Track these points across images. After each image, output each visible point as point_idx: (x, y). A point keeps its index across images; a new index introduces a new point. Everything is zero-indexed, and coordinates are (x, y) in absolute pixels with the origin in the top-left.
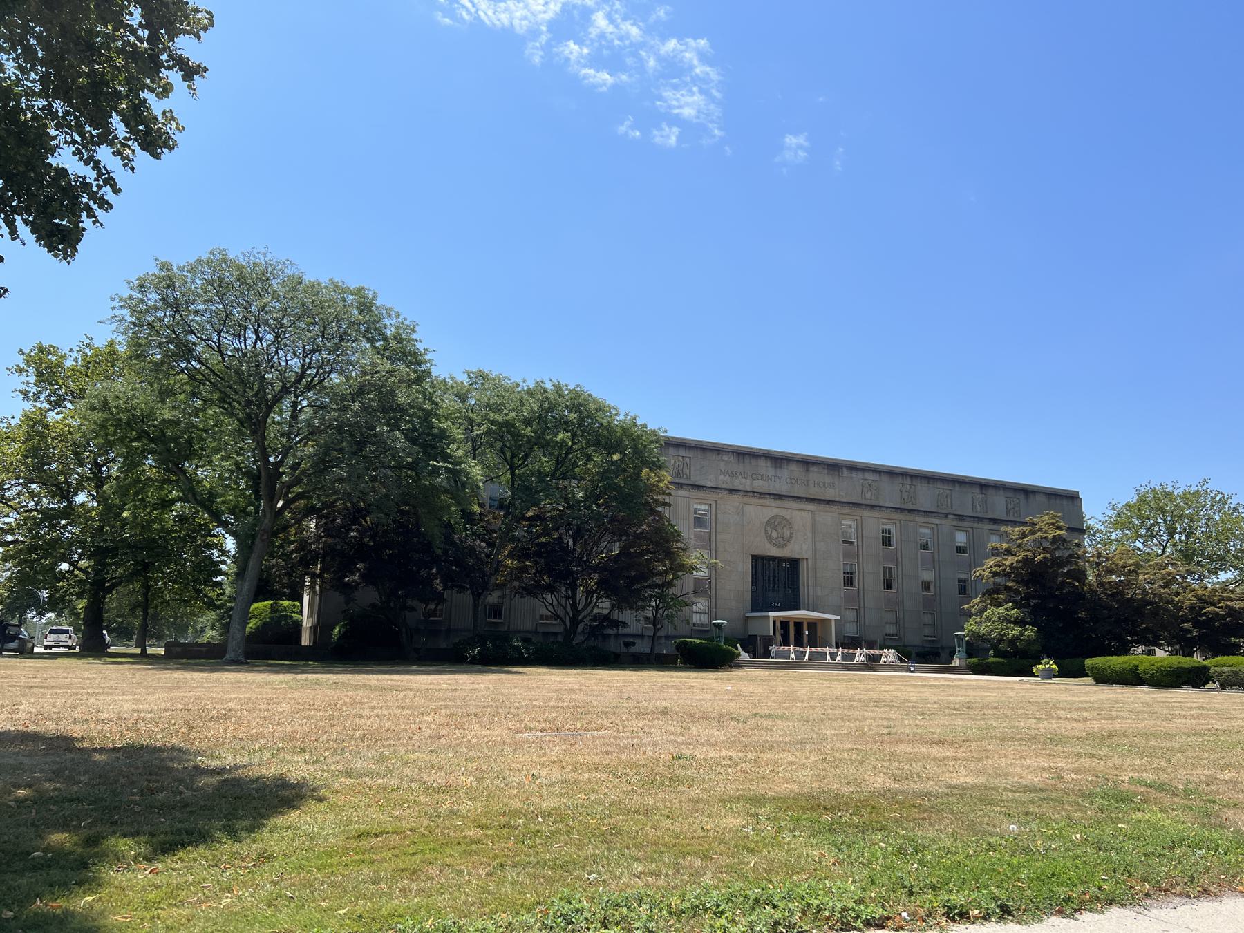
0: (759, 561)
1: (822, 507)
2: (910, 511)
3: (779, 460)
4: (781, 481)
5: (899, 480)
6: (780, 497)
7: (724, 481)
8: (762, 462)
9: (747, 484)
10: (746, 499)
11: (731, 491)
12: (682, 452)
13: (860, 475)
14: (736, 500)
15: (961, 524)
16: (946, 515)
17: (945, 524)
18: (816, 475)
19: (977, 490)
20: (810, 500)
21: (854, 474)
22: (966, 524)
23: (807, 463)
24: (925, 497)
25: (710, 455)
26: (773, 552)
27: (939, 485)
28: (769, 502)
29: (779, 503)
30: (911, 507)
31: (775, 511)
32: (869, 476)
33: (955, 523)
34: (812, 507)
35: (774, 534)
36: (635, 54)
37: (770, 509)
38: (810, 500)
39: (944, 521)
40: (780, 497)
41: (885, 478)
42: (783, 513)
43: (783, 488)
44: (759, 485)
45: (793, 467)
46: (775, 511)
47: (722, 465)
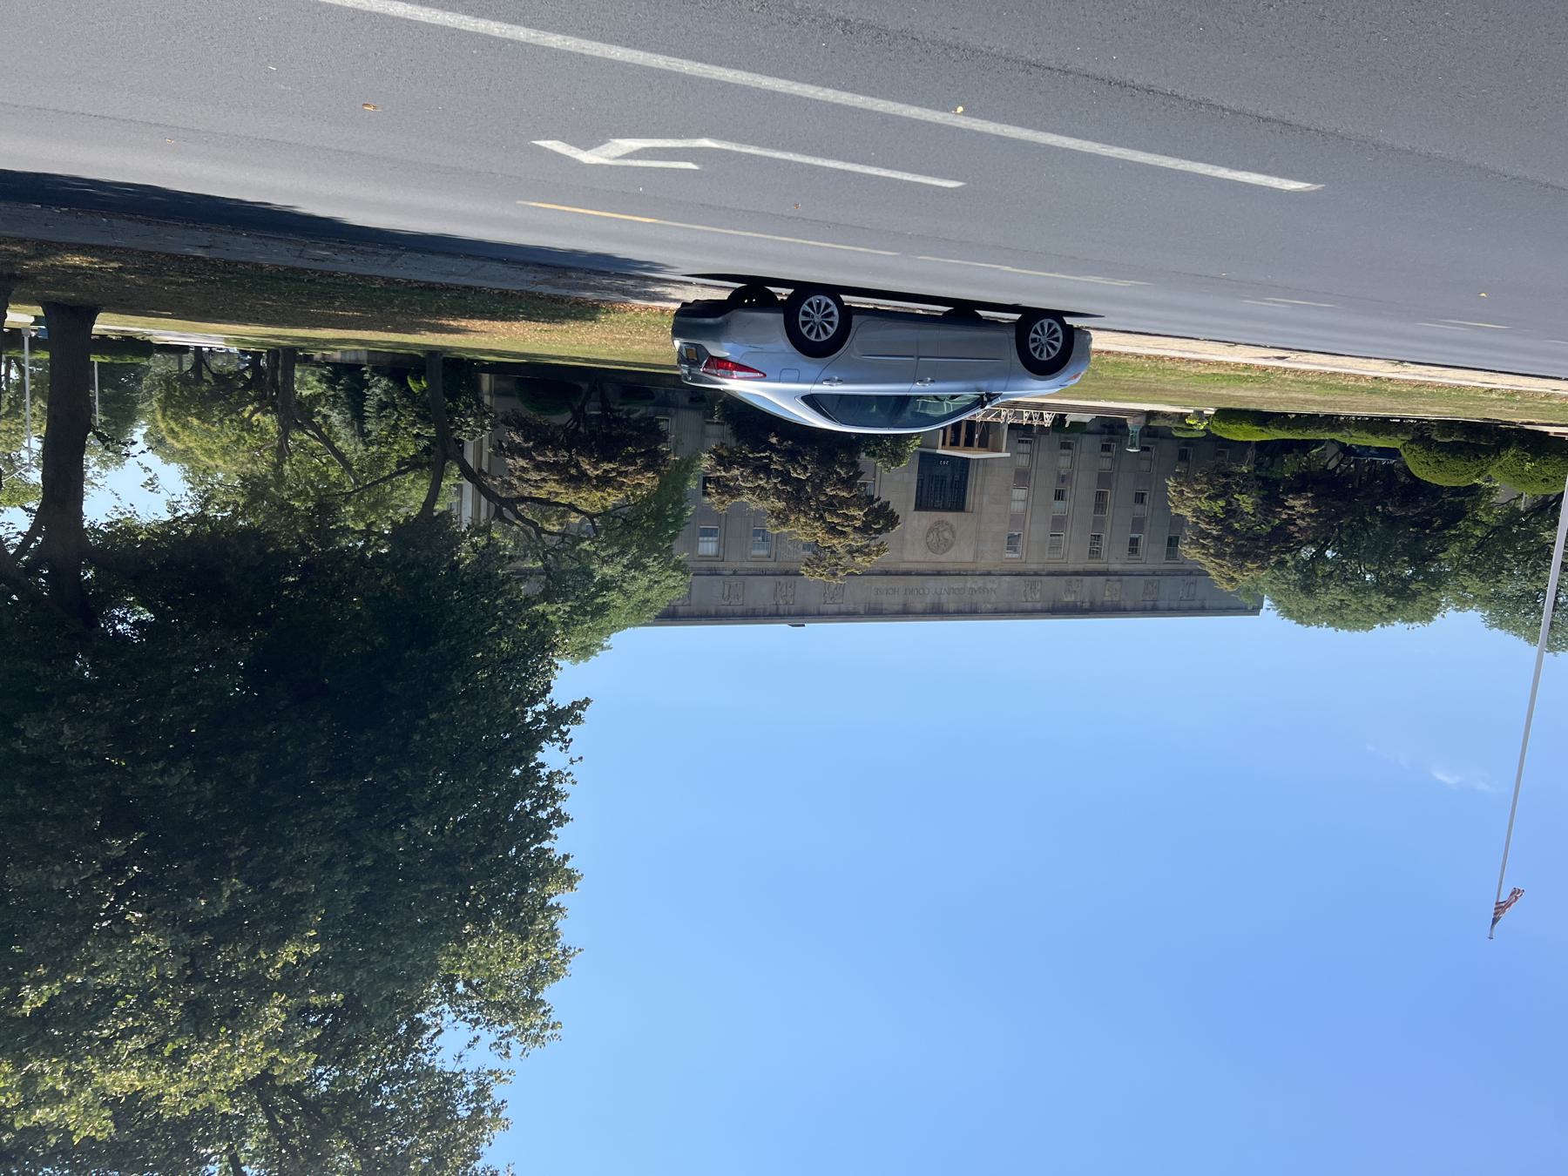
0: (958, 505)
1: (892, 568)
2: (787, 573)
3: (937, 612)
4: (934, 589)
5: (793, 609)
6: (939, 574)
7: (992, 583)
8: (952, 607)
9: (971, 583)
10: (973, 567)
11: (989, 574)
12: (1029, 606)
13: (843, 608)
14: (983, 565)
15: (713, 565)
16: (735, 573)
17: (734, 562)
18: (895, 601)
19: (681, 609)
20: (907, 573)
21: (851, 607)
22: (705, 565)
23: (905, 613)
24: (761, 592)
25: (1002, 606)
26: (949, 517)
27: (738, 609)
28: (949, 567)
29: (940, 567)
30: (782, 579)
31: (943, 558)
32: (832, 608)
33: (721, 565)
34: (904, 567)
35: (947, 534)
36: (455, 954)
37: (948, 559)
38: (907, 573)
39: (738, 565)
40: (939, 574)
41: (813, 609)
42: (931, 556)
43: (933, 583)
44: (956, 583)
45: (919, 606)
46: (943, 558)
47: (993, 598)
